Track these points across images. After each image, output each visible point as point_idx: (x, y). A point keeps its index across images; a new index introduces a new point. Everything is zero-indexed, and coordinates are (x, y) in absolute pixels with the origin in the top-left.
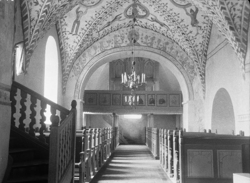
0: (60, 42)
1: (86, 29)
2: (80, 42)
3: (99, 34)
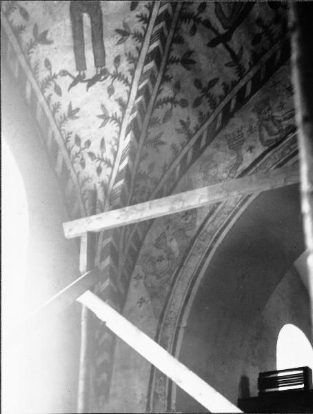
0: (49, 142)
1: (138, 26)
2: (129, 110)
3: (236, 59)
